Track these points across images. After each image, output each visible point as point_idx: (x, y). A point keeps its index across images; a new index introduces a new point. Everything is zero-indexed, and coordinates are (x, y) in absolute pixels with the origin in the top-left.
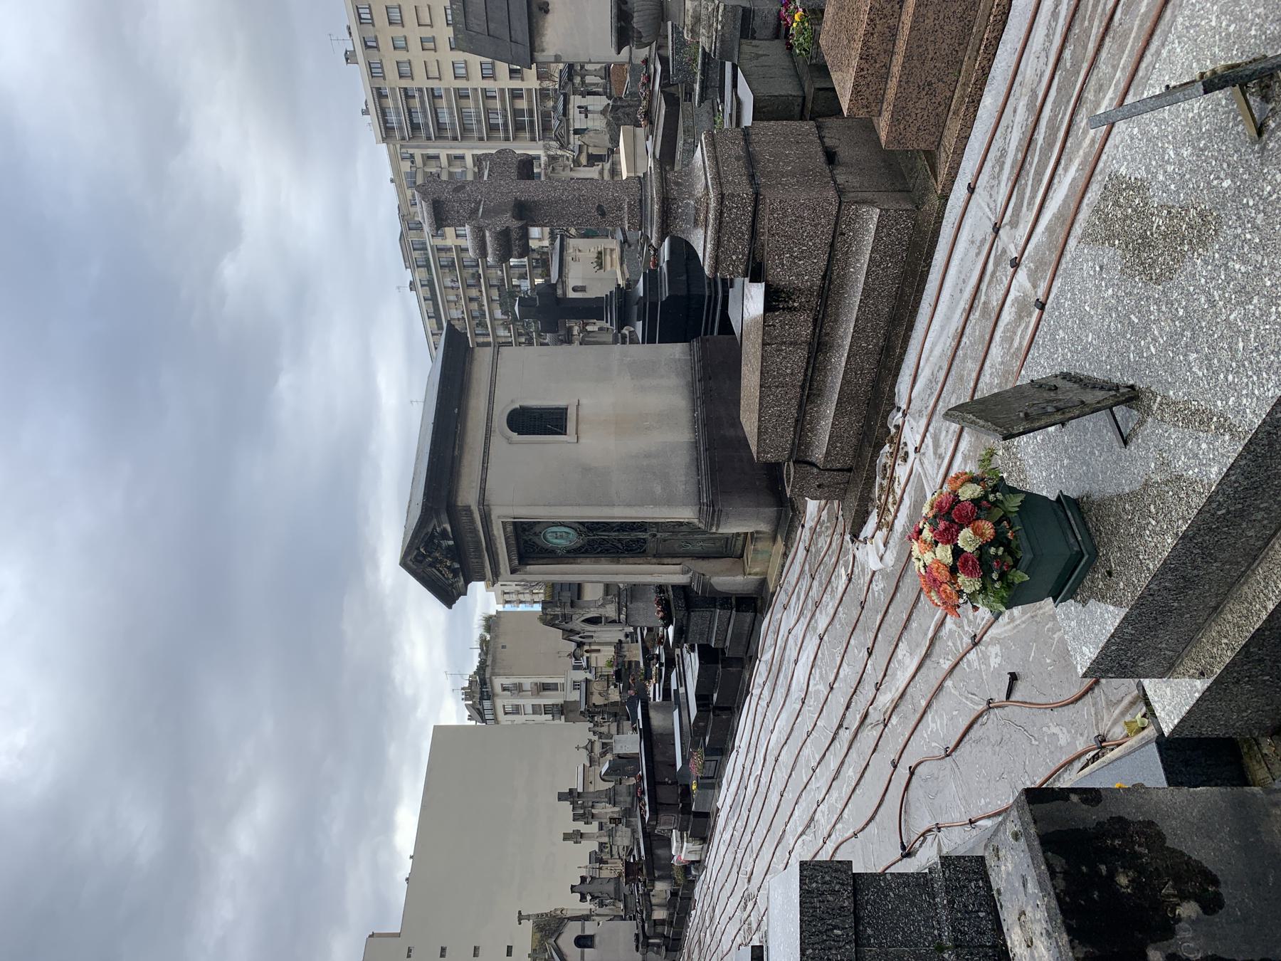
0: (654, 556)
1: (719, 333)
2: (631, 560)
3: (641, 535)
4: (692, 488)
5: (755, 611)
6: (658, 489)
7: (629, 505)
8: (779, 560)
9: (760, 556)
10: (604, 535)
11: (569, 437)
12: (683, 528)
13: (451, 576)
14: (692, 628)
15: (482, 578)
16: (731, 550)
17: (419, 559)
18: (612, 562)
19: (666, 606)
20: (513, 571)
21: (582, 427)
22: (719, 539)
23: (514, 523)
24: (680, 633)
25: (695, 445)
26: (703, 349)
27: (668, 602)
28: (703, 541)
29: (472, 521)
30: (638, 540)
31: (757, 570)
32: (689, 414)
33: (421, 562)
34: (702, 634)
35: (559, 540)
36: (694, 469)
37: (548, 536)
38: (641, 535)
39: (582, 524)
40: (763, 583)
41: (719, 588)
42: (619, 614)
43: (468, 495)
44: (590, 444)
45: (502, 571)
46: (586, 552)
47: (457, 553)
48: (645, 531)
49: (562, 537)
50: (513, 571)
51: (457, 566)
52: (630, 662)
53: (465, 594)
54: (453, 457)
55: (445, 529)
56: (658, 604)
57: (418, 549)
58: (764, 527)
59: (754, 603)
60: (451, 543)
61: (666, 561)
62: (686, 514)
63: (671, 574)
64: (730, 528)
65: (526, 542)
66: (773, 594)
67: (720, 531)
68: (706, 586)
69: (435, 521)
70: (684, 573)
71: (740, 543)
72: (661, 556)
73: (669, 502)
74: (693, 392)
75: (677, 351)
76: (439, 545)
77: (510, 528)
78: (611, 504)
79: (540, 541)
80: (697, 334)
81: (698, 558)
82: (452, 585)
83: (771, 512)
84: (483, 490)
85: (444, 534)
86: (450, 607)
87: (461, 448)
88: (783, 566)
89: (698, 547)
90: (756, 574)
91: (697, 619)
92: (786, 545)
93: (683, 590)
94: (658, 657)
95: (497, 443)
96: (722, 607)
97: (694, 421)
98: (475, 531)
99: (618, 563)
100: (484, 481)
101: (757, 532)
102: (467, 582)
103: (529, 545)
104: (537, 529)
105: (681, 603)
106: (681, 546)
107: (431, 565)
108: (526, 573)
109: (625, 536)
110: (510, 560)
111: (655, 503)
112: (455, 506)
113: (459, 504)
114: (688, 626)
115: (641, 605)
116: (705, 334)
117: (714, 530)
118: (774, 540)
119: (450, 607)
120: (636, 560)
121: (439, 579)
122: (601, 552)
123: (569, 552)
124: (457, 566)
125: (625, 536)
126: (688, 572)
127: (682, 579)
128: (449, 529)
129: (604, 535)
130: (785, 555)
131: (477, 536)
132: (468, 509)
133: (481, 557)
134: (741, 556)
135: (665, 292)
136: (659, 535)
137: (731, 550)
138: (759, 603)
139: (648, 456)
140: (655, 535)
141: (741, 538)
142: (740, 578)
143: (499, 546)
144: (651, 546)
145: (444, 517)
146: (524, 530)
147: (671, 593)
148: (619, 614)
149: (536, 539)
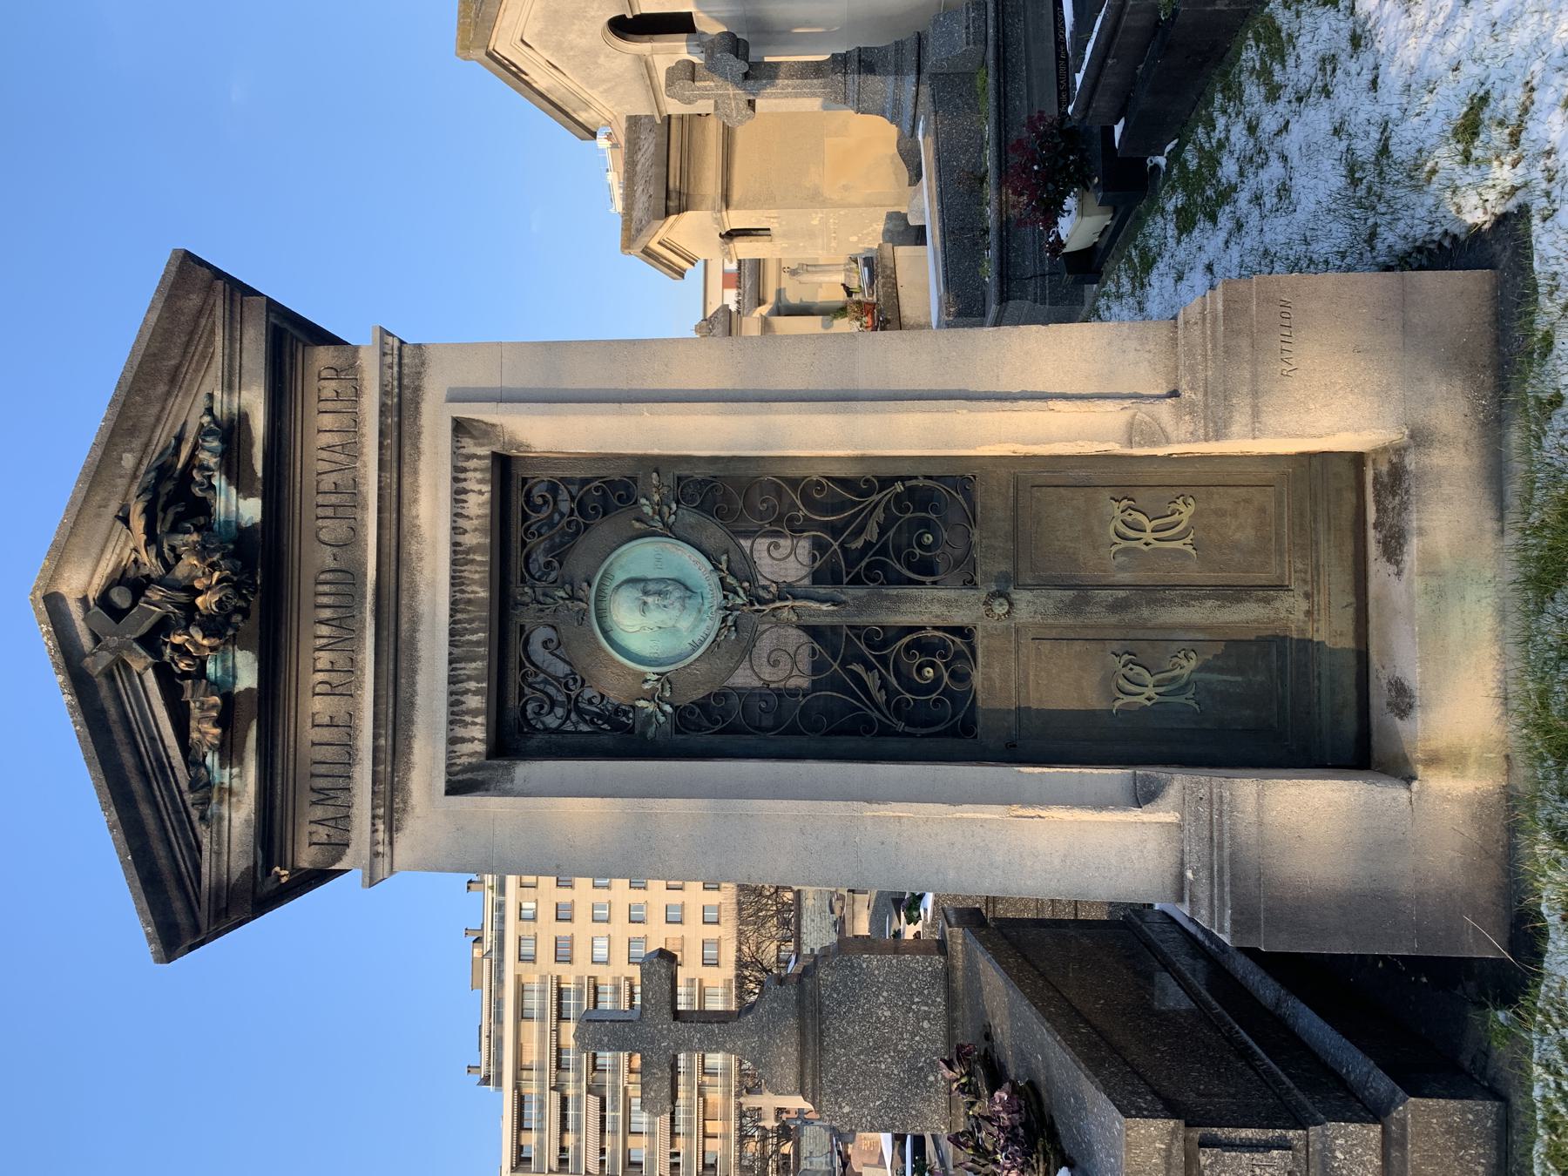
33: (117, 614)
77: (478, 502)
110: (456, 715)
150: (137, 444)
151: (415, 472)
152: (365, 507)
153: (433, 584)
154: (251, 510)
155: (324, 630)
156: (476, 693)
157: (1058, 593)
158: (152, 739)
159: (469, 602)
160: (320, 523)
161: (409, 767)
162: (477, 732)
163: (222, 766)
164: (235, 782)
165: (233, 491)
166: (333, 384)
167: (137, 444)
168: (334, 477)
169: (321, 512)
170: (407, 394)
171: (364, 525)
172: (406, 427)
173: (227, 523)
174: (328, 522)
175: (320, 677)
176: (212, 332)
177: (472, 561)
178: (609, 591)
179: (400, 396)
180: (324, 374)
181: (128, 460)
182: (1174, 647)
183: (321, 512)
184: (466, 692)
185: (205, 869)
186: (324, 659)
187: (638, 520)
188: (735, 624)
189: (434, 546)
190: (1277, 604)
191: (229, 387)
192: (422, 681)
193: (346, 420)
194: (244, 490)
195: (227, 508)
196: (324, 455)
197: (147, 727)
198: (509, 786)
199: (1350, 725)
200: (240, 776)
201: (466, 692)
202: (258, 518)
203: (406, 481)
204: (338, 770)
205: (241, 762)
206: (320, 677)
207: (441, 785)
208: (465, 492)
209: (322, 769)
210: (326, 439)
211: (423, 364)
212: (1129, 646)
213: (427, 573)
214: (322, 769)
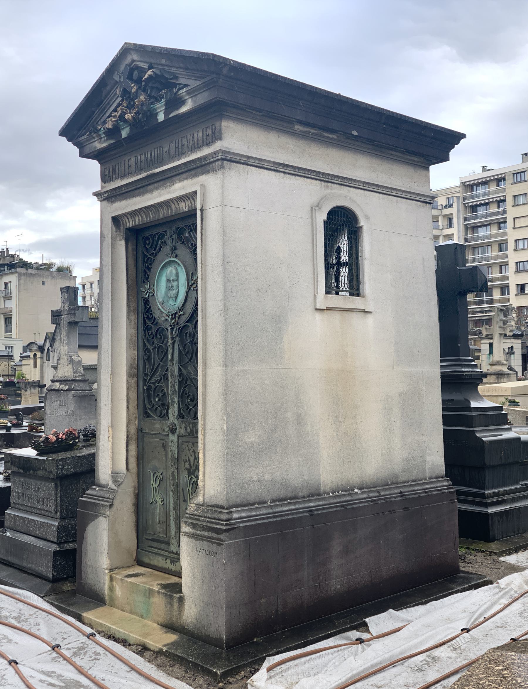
0: (140, 430)
1: (460, 512)
2: (134, 395)
3: (173, 411)
4: (255, 492)
5: (54, 580)
6: (252, 437)
7: (226, 391)
8: (134, 636)
9: (139, 598)
10: (173, 354)
11: (323, 300)
12: (184, 476)
13: (109, 125)
14: (34, 483)
15: (105, 178)
16: (150, 546)
17: (133, 73)
18: (131, 367)
19: (66, 444)
20: (116, 220)
21: (337, 316)
22: (167, 531)
23: (192, 214)
24: (24, 463)
25: (315, 494)
26: (441, 495)
27: (71, 447)
28: (164, 505)
29: (196, 147)
30: (165, 407)
31: (119, 592)
32: (356, 480)
33: (130, 77)
34: (23, 496)
35: (167, 288)
36: (282, 494)
37: (170, 270)
38: (173, 411)
39: (193, 317)
40: (97, 599)
41: (90, 529)
42: (61, 382)
43: (236, 137)
44: (313, 332)
45: (117, 205)
46: (147, 328)
47: (146, 131)
48: (181, 416)
49: (170, 288)
50: (116, 220)
51: (125, 133)
52: (20, 395)
53: (82, 155)
54: (291, 122)
55: (183, 102)
56: (69, 434)
57: (151, 67)
58: (190, 613)
59: (66, 582)
60: (161, 117)
61: (133, 447)
62: (212, 484)
63: (112, 456)
64: (190, 557)
65: (161, 236)
66: (79, 618)
67: (184, 540)
68: (92, 511)
69: (194, 83)
70: (114, 475)
71: (160, 562)
72: (141, 442)
73: (232, 456)
74: (385, 484)
75: (435, 458)
76: (157, 100)
77: (184, 207)
78: (227, 362)
79: (164, 256)
80: (455, 482)
81: (137, 496)
82: (97, 131)
83: (219, 626)
84: (246, 161)
85: (175, 102)
86: (64, 132)
87: (303, 136)
88: (124, 643)
89: (155, 497)
90: (112, 589)
91: (47, 491)
92: (160, 653)
93: (87, 470)
94: (18, 425)
95: (310, 191)
96: (61, 529)
97: (348, 490)
98: (180, 154)
99: (130, 375)
100: (260, 164)
101: (181, 600)
102: (97, 155)
103: (154, 241)
104: (183, 251)
105: (69, 469)
106: (155, 470)
107: (126, 93)
108: (113, 239)
109: (172, 386)
110: (133, 214)
111: (232, 433)
112: (221, 116)
113: (225, 124)
114: (36, 477)
115: (72, 407)
116: (459, 493)
117: (185, 528)
118: (170, 627)
119: (64, 132)
120: (134, 403)
121: (104, 111)
122: (147, 350)
123: (146, 301)
124: (125, 133)
125: (172, 386)
126: (115, 481)
127: (104, 471)
128: (184, 109)
129: (173, 354)
130: (142, 650)
131: (172, 158)
132: (217, 136)
133: (139, 170)
134: (139, 563)
135: (487, 436)
136: (173, 438)
137: (150, 546)
138: (67, 586)
139: (300, 421)
140: (173, 431)
141: (168, 565)
142: (105, 562)
143: (156, 193)
144: (157, 425)
145: (203, 98)
146: (180, 232)
147: (85, 452)
148: (61, 382)
149: (166, 249)
150: (168, 63)
151: (187, 178)
152: (179, 160)
153: (160, 196)
154: (161, 117)
155: (149, 155)
156: (139, 220)
157: (176, 453)
158: (109, 103)
159: (159, 211)
160: (174, 142)
161: (120, 200)
162: (130, 224)
163: (104, 133)
164: (103, 139)
165: (164, 108)
166: (210, 133)
167: (168, 63)
168: (186, 143)
169: (177, 140)
170: (208, 167)
171: (186, 157)
172: (199, 170)
173: (156, 110)
174: (174, 144)
175: (139, 157)
176: (204, 78)
177: (168, 209)
178: (175, 265)
179: (206, 164)
180: (213, 127)
181: (163, 61)
182: (164, 497)
183: (177, 140)
184: (139, 217)
185: (83, 138)
186: (143, 157)
187: (192, 274)
188: (166, 320)
189: (169, 193)
190: (175, 540)
191: (188, 93)
192: (137, 199)
193: (200, 142)
194: (167, 112)
195: (158, 108)
196: (191, 137)
197: (111, 100)
198: (118, 239)
199: (146, 560)
200: (105, 141)
201: (139, 217)
202: (159, 121)
203: (184, 175)
204: (120, 175)
205: (107, 140)
206: (139, 157)
207: (113, 215)
208: (184, 201)
209: (120, 167)
210: (196, 135)
211: (216, 171)
212: (164, 478)
213: (163, 192)
214: (120, 167)
